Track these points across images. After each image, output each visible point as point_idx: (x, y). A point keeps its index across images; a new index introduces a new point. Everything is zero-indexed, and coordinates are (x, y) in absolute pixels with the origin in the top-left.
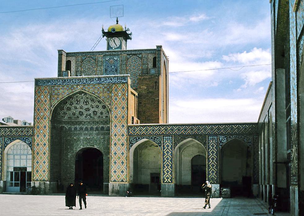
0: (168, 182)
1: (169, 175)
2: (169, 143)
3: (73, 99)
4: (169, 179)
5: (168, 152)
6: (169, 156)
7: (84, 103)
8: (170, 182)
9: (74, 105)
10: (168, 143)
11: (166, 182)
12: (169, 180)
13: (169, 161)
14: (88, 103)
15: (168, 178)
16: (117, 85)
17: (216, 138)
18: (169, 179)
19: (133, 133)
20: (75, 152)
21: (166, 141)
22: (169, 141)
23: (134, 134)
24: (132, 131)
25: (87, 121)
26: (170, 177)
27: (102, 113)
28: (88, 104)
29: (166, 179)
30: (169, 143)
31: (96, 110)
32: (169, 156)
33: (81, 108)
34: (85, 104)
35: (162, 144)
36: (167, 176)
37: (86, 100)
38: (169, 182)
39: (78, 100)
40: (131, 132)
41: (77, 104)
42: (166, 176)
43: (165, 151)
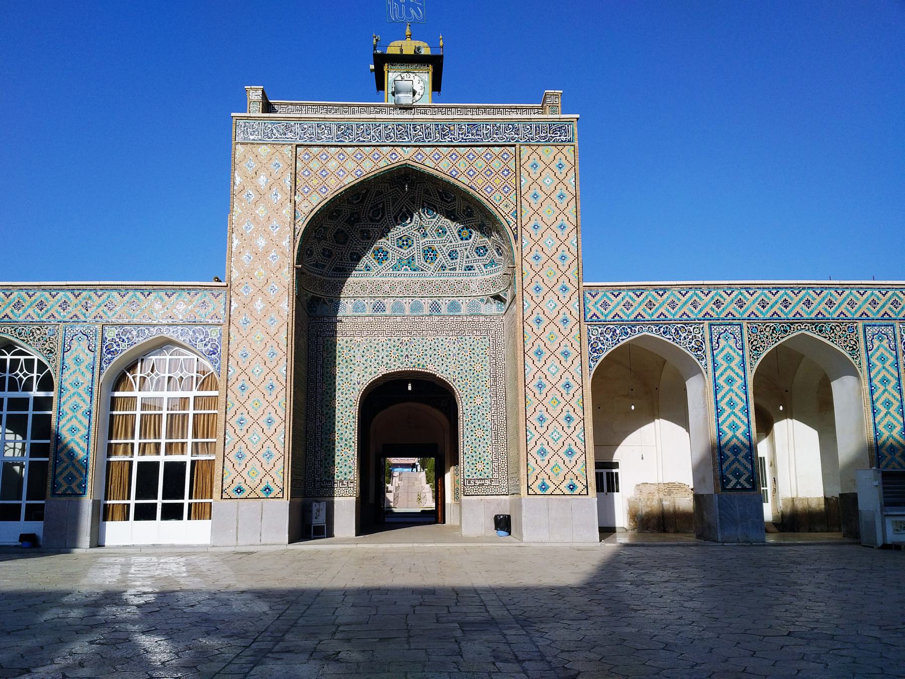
0: (739, 487)
1: (744, 461)
2: (731, 347)
4: (744, 477)
5: (730, 381)
6: (737, 395)
8: (747, 486)
10: (728, 350)
11: (734, 489)
12: (742, 480)
13: (736, 411)
15: (737, 475)
16: (540, 150)
17: (889, 331)
18: (744, 477)
19: (602, 314)
20: (358, 387)
21: (722, 342)
22: (732, 342)
23: (606, 316)
24: (598, 305)
25: (400, 283)
26: (746, 468)
27: (452, 255)
29: (730, 477)
30: (731, 347)
32: (737, 395)
35: (709, 354)
36: (734, 466)
37: (404, 210)
38: (744, 489)
39: (380, 206)
40: (594, 311)
41: (372, 220)
42: (730, 465)
43: (722, 374)
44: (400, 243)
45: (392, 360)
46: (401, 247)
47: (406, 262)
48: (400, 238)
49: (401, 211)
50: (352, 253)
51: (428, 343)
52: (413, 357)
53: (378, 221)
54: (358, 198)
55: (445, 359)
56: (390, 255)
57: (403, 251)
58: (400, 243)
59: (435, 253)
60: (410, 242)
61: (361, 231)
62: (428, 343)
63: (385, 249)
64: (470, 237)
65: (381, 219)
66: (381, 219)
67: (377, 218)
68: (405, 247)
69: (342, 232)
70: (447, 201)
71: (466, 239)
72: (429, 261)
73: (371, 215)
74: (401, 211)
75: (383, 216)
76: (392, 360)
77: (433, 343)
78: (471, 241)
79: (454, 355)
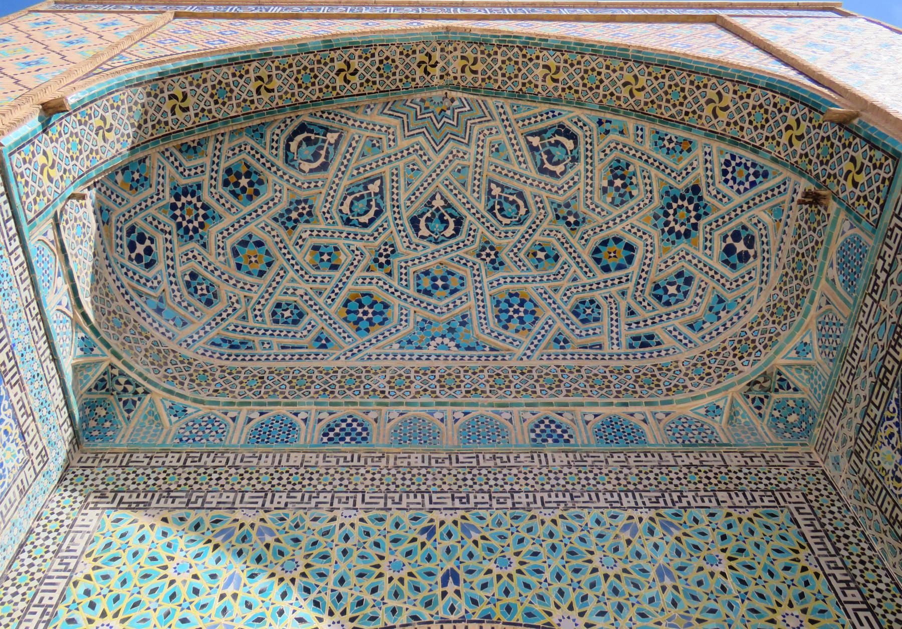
3: (324, 167)
7: (415, 222)
9: (325, 228)
14: (457, 231)
27: (586, 311)
28: (450, 231)
31: (530, 290)
33: (383, 260)
34: (424, 231)
37: (438, 203)
39: (374, 188)
41: (348, 222)
44: (426, 283)
45: (386, 588)
46: (427, 293)
47: (444, 328)
48: (427, 273)
49: (429, 204)
50: (279, 305)
51: (541, 531)
52: (480, 578)
53: (365, 225)
54: (316, 156)
55: (624, 587)
56: (394, 313)
57: (432, 300)
58: (426, 283)
59: (529, 306)
60: (453, 282)
61: (316, 248)
62: (541, 531)
63: (381, 295)
64: (630, 259)
65: (372, 221)
66: (372, 221)
67: (364, 219)
68: (437, 293)
69: (259, 244)
70: (553, 174)
71: (620, 267)
72: (515, 324)
73: (346, 209)
74: (429, 204)
75: (378, 213)
76: (386, 588)
77: (560, 530)
78: (634, 269)
79: (662, 572)
